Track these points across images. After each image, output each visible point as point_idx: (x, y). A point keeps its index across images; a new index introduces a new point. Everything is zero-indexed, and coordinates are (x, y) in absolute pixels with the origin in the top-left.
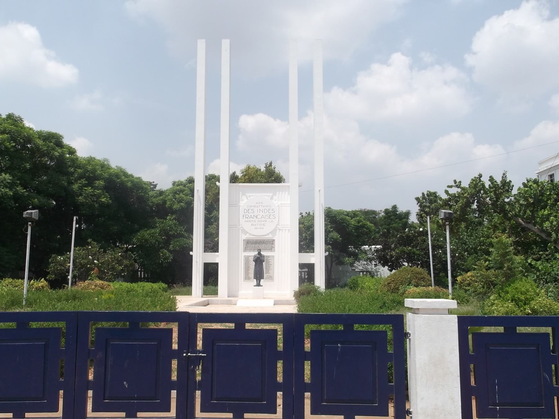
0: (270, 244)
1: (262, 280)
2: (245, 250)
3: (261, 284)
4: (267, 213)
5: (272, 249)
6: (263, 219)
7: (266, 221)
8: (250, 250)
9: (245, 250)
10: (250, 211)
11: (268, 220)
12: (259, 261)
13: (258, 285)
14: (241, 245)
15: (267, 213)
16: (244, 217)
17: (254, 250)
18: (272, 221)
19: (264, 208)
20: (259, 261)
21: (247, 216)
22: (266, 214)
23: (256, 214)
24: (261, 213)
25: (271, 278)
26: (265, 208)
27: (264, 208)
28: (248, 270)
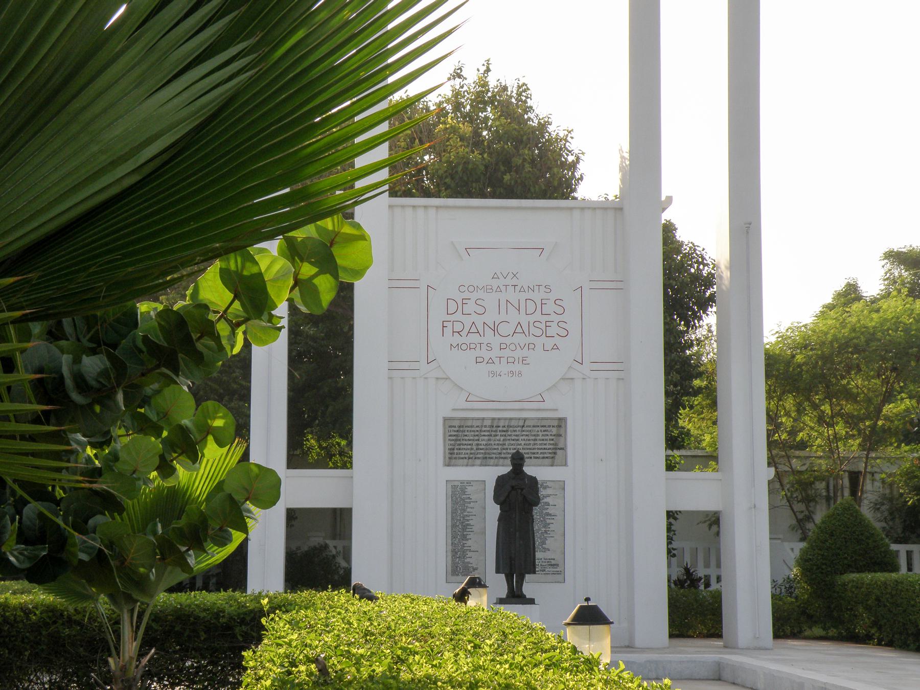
0: (552, 437)
1: (528, 577)
2: (452, 457)
3: (528, 589)
4: (537, 316)
5: (555, 453)
6: (520, 339)
7: (531, 346)
8: (471, 460)
9: (452, 457)
10: (470, 307)
11: (539, 342)
12: (519, 499)
13: (515, 596)
14: (435, 443)
15: (537, 316)
16: (449, 331)
17: (486, 460)
18: (555, 347)
19: (523, 296)
20: (519, 499)
21: (458, 327)
22: (532, 319)
23: (489, 318)
24: (514, 317)
25: (556, 569)
26: (531, 295)
27: (523, 296)
28: (464, 537)
